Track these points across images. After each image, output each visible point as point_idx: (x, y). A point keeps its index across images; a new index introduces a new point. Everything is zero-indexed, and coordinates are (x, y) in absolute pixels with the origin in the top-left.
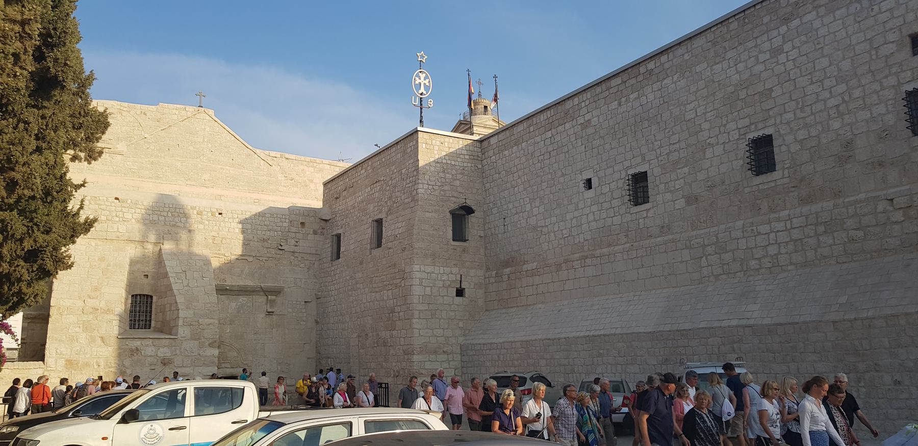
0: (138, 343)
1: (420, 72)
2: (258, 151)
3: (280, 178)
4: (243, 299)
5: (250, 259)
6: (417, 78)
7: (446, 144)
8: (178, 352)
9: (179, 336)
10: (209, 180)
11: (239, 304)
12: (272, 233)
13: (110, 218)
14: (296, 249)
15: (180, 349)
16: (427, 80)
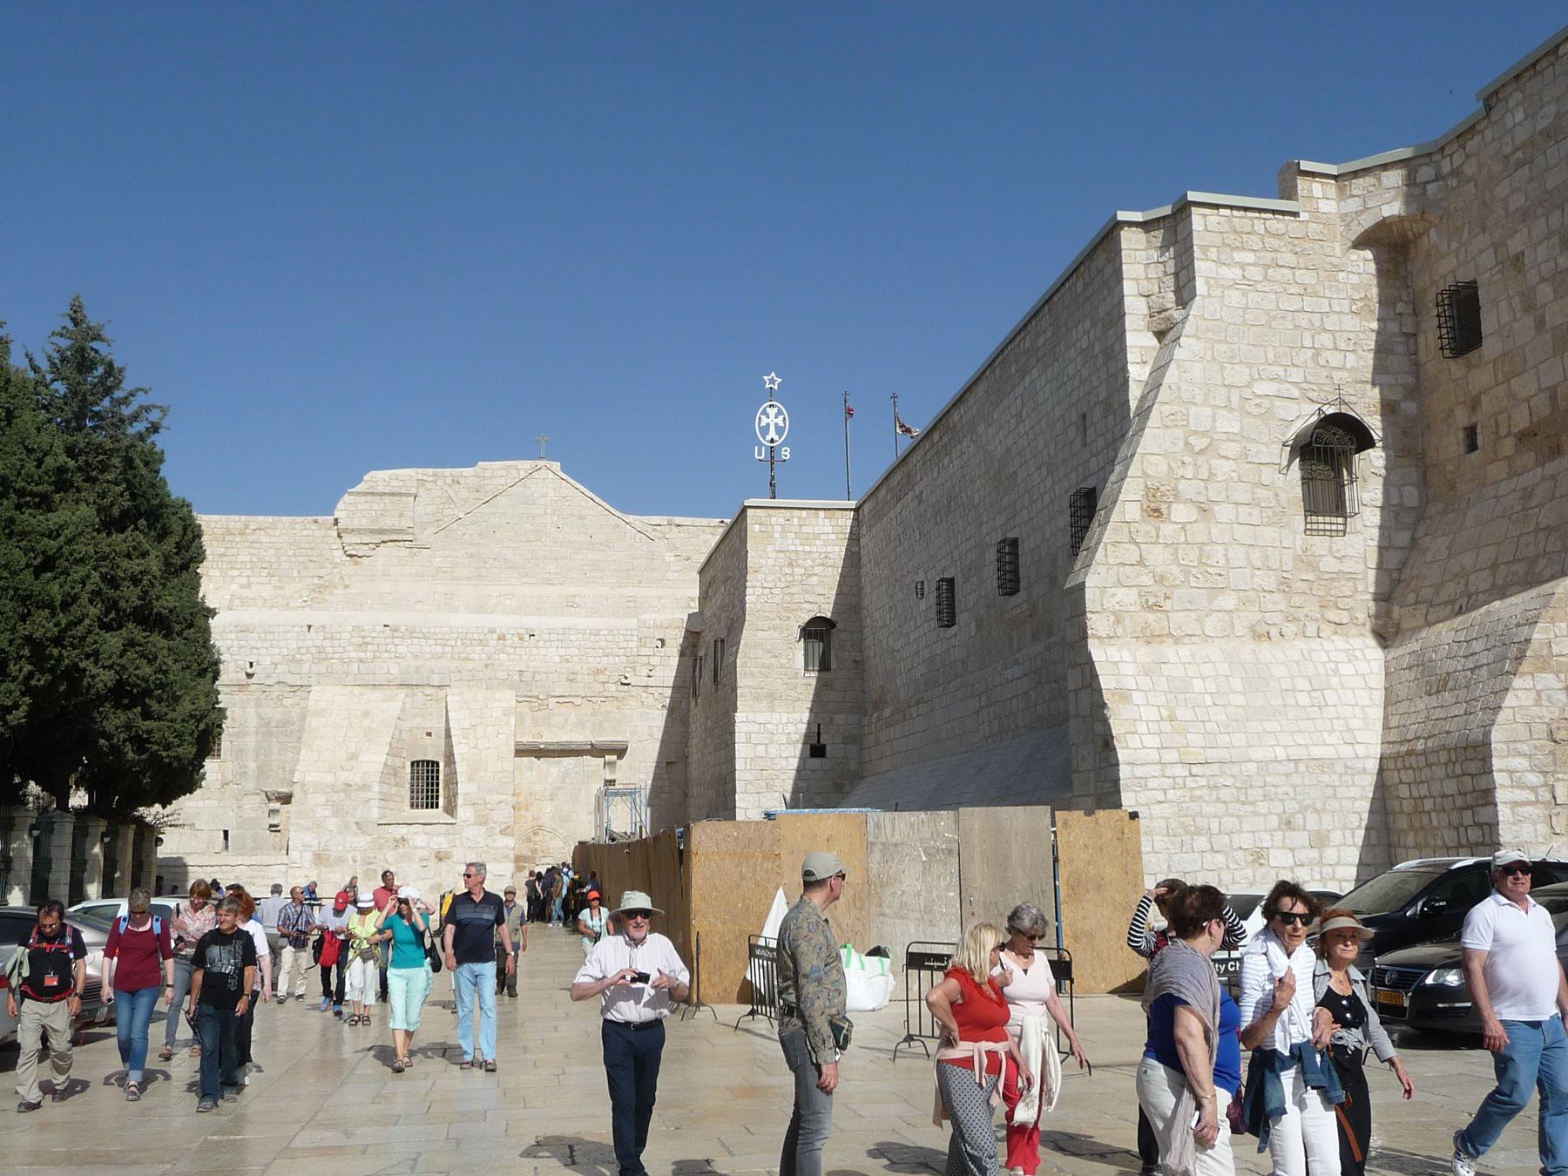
0: (404, 830)
1: (771, 406)
2: (630, 518)
3: (667, 559)
4: (568, 762)
5: (578, 701)
6: (763, 417)
7: (796, 520)
8: (458, 842)
9: (458, 819)
10: (556, 573)
11: (563, 769)
12: (611, 659)
13: (378, 655)
14: (651, 682)
15: (461, 837)
16: (781, 417)
